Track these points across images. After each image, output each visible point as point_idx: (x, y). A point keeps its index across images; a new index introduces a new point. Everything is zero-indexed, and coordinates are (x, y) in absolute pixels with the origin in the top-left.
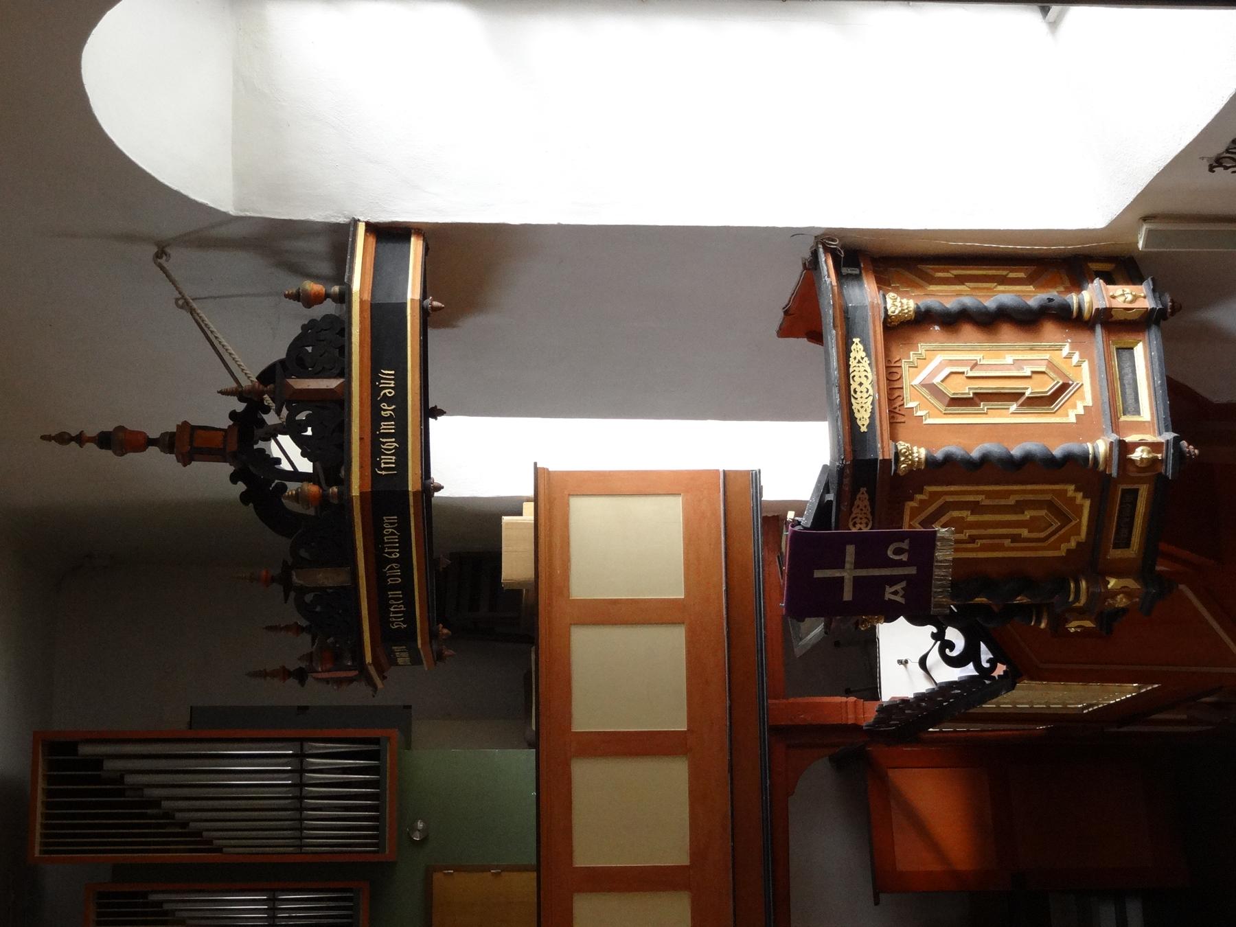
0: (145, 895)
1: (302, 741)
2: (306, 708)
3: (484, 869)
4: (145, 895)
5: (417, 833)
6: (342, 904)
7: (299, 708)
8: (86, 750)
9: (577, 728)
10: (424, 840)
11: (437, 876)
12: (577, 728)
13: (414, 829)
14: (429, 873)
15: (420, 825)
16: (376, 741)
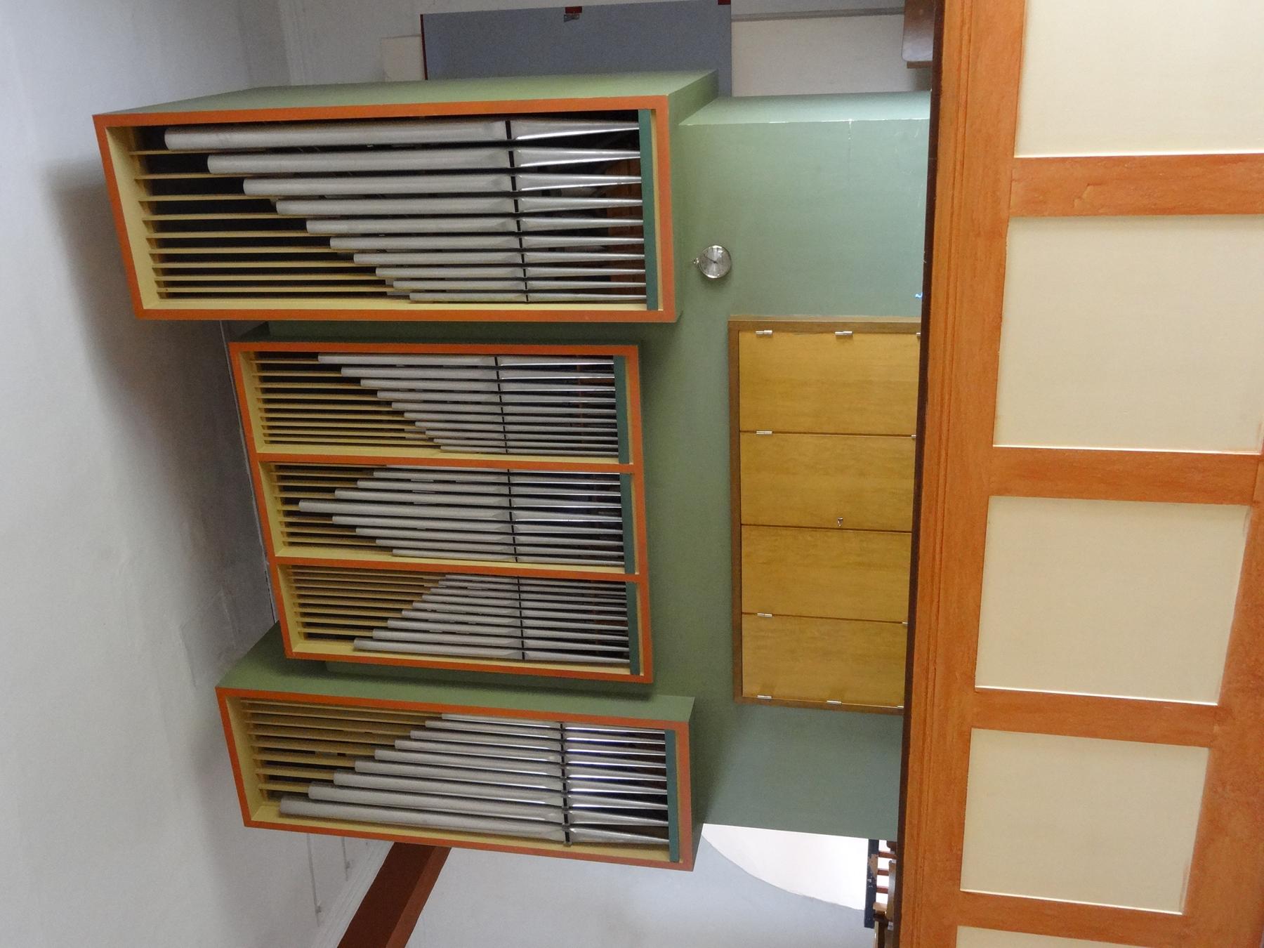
0: (314, 355)
1: (508, 118)
2: (579, 9)
3: (828, 328)
4: (314, 355)
5: (714, 267)
6: (599, 376)
7: (569, 10)
8: (177, 142)
9: (1024, 152)
10: (723, 280)
11: (746, 338)
12: (1024, 152)
13: (706, 260)
14: (734, 331)
15: (717, 251)
16: (631, 115)
